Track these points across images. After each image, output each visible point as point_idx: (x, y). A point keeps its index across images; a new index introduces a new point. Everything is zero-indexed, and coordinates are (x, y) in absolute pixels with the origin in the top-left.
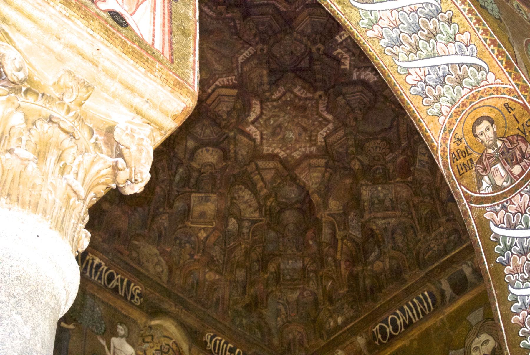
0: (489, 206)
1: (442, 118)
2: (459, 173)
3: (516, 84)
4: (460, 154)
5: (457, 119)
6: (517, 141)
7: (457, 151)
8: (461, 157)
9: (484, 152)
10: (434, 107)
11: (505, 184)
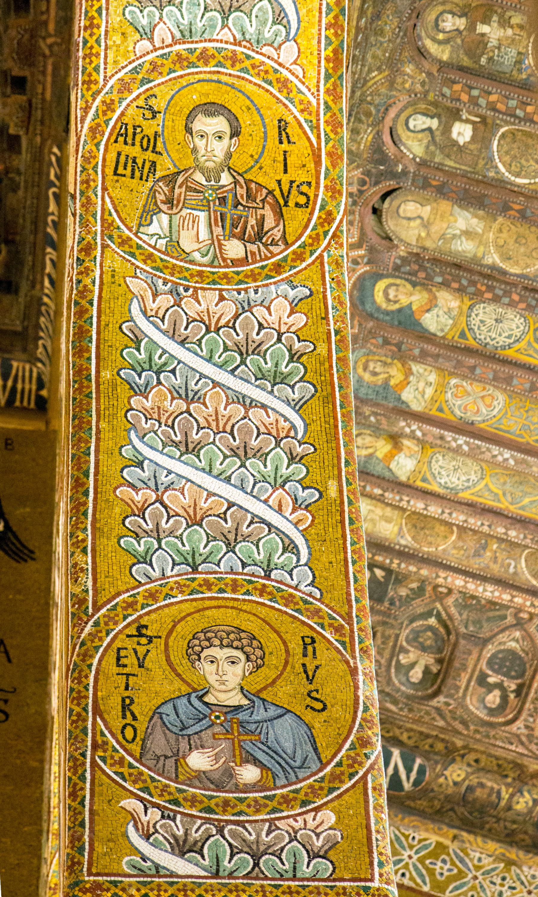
0: (145, 271)
1: (146, 45)
2: (116, 168)
3: (326, 103)
4: (138, 138)
5: (174, 71)
6: (263, 201)
7: (135, 128)
8: (138, 143)
9: (186, 170)
10: (145, 12)
11: (197, 256)
